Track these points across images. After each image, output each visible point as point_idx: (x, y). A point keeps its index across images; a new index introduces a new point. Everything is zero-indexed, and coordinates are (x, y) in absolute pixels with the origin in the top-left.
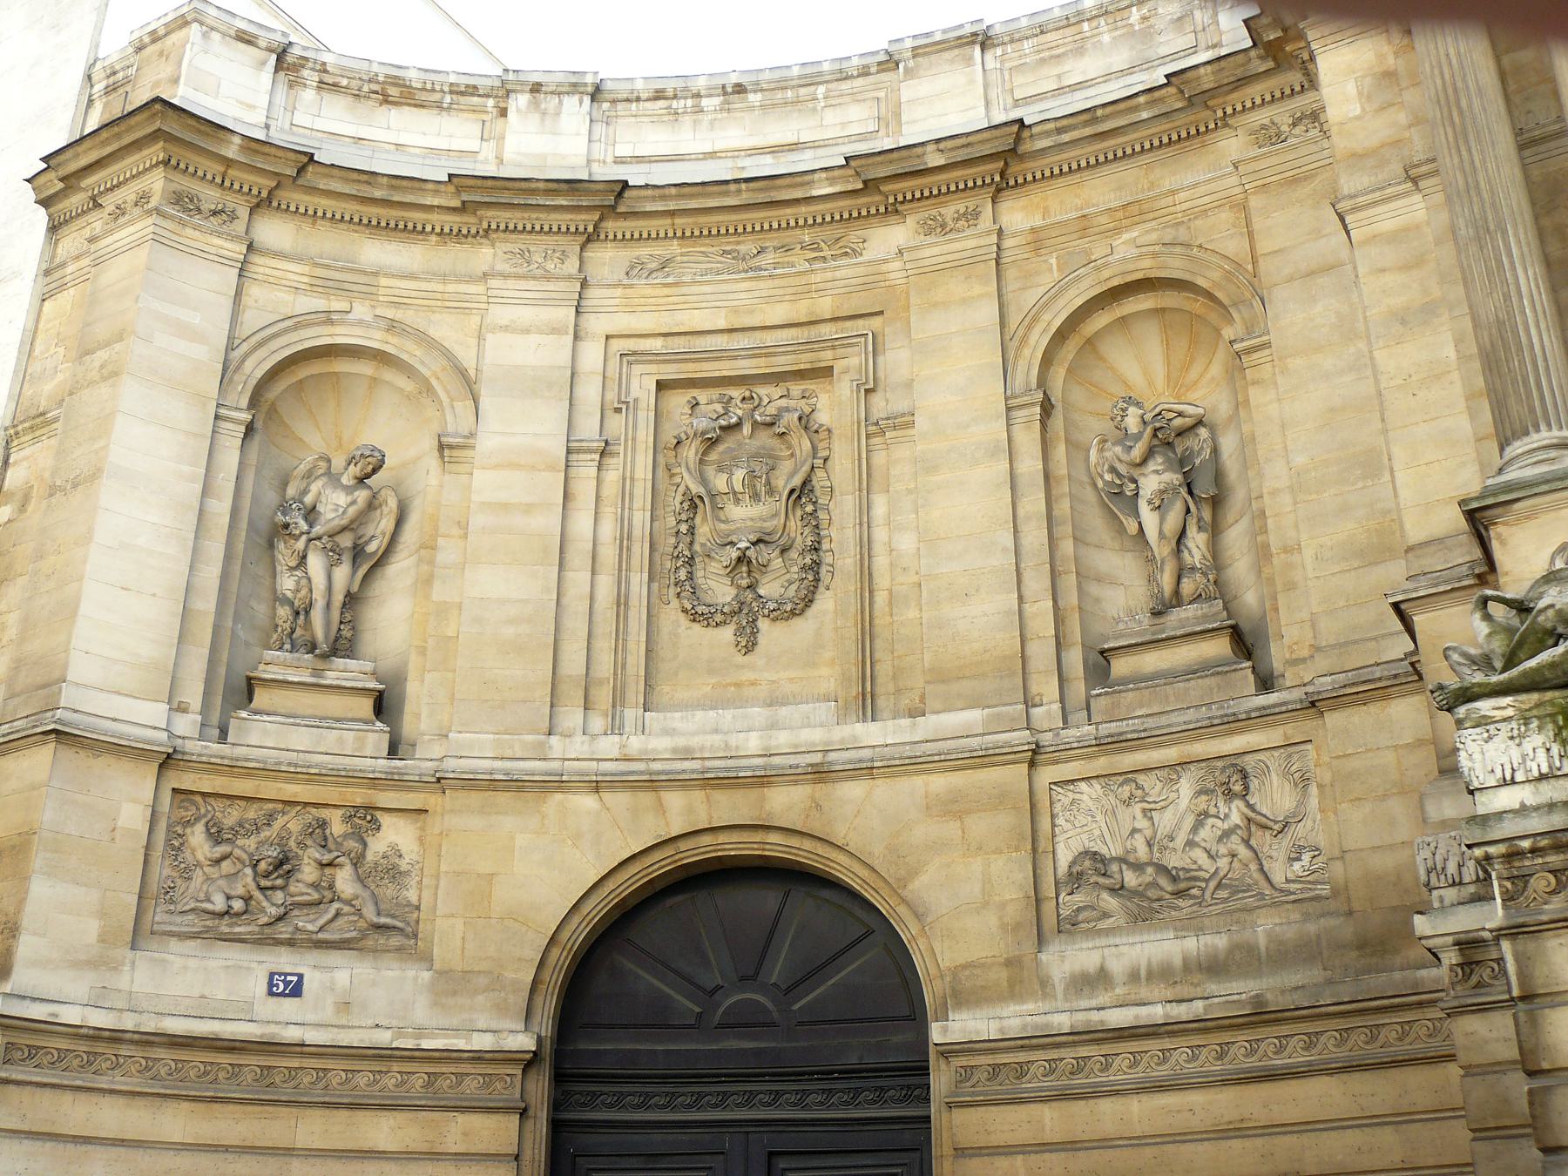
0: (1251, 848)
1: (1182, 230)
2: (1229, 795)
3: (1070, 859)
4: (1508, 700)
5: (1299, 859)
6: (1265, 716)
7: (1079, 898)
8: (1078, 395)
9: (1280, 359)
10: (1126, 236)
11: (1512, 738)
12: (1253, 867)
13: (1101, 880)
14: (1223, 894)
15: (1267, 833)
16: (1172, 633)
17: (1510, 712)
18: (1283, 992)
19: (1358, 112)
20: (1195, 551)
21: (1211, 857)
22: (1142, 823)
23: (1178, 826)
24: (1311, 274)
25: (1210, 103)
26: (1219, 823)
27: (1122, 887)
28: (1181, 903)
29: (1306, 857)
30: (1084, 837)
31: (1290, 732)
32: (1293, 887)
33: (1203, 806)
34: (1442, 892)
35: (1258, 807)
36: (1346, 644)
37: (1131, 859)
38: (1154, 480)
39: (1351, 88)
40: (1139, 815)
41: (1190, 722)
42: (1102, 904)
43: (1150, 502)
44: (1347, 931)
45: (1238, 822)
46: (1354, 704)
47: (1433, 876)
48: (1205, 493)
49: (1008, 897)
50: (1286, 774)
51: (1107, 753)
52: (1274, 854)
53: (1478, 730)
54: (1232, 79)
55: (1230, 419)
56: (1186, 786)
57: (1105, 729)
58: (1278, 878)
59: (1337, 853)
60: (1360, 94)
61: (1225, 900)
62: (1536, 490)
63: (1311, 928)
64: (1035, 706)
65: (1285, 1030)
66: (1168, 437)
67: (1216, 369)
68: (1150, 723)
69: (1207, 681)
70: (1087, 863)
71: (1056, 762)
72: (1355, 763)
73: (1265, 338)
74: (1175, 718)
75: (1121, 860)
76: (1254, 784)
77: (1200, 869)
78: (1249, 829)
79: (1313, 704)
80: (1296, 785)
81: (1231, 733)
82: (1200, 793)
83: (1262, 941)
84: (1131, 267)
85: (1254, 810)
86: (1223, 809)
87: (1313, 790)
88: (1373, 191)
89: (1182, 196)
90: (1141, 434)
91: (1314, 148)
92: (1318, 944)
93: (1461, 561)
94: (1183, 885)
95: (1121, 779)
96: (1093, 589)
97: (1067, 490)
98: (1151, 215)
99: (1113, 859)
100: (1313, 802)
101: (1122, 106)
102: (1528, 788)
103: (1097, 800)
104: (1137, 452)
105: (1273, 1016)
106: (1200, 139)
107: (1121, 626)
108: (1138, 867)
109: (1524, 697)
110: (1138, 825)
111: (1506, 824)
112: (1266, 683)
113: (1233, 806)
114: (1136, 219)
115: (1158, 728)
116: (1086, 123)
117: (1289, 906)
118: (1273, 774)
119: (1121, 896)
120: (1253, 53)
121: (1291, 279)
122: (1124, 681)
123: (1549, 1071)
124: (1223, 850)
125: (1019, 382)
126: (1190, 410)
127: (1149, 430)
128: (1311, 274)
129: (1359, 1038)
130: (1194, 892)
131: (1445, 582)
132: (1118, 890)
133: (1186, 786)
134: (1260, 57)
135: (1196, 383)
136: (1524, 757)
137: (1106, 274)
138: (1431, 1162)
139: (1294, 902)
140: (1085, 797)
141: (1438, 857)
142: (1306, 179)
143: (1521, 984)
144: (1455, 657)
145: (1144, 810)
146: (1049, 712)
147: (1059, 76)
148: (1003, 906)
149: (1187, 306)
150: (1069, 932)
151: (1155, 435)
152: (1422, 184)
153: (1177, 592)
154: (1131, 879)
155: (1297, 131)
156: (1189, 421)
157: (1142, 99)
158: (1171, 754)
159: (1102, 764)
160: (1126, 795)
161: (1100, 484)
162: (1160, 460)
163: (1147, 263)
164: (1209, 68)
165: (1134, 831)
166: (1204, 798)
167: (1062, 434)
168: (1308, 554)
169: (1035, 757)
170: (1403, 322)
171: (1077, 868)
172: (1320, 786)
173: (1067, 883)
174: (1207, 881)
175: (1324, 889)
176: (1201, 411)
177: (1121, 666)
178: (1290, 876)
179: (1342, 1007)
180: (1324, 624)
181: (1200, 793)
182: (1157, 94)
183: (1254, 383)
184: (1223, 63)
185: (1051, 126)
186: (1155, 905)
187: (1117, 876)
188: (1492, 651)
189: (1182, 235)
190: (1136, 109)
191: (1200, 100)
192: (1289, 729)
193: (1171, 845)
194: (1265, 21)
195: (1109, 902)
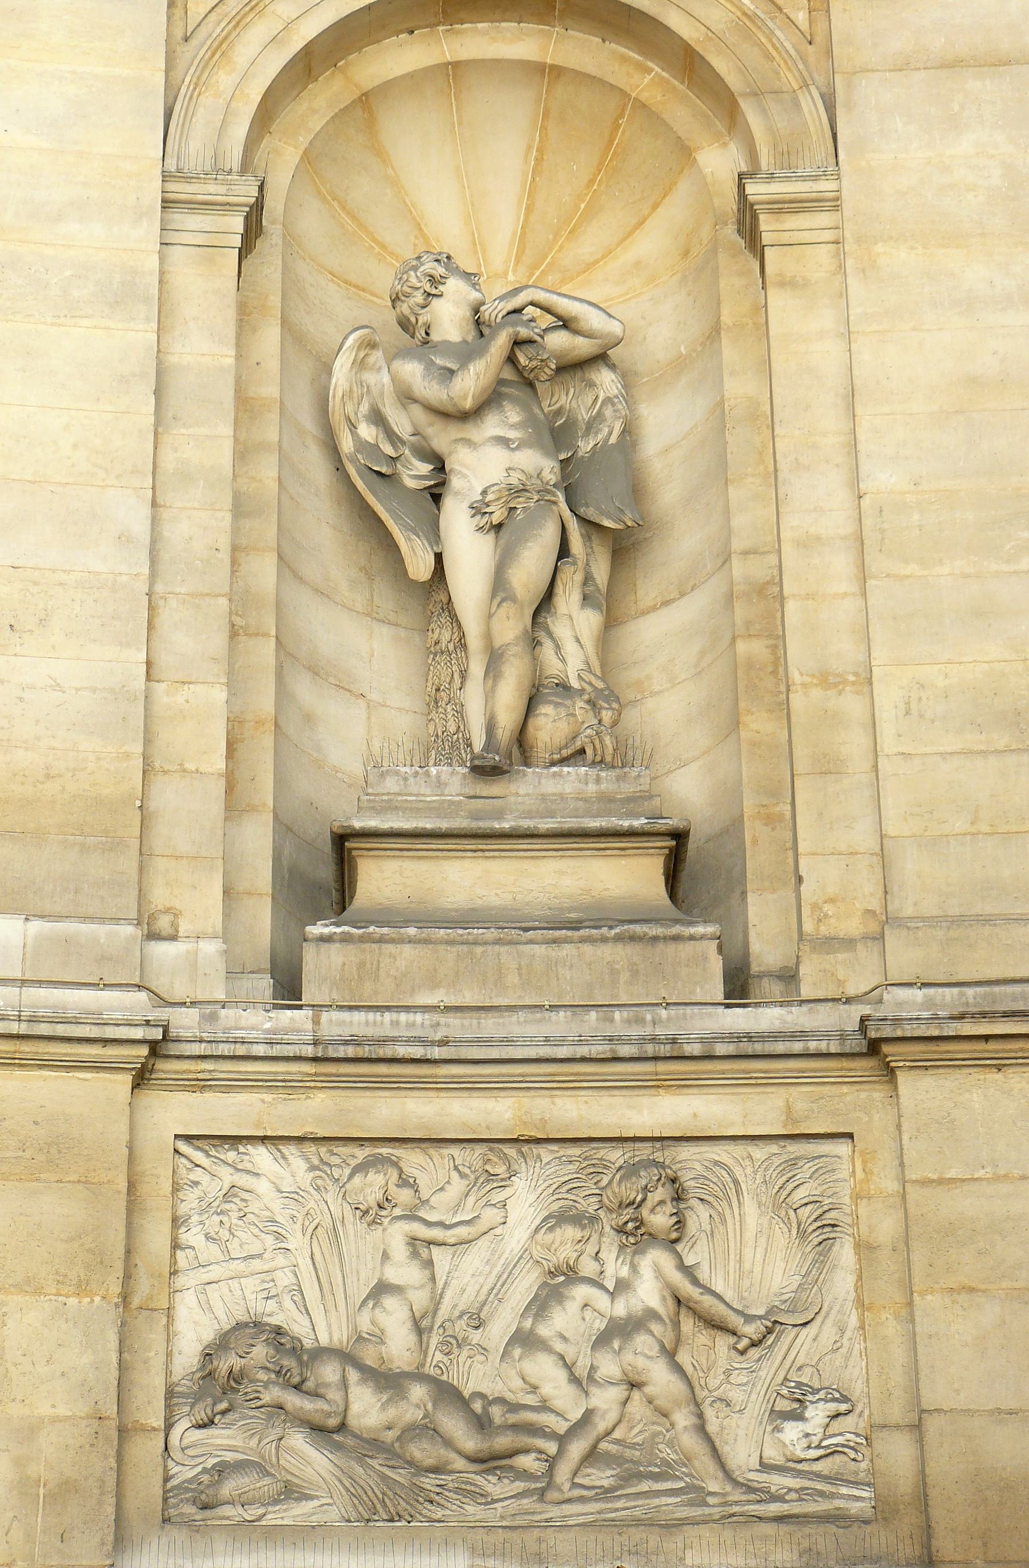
0: (678, 1369)
2: (635, 1235)
3: (208, 1334)
5: (797, 1416)
7: (227, 1440)
8: (313, 223)
9: (859, 240)
12: (683, 1419)
13: (293, 1400)
14: (602, 1477)
15: (724, 1342)
16: (527, 824)
20: (570, 648)
21: (575, 1380)
22: (404, 1272)
23: (497, 1292)
24: (953, 64)
26: (602, 1301)
27: (342, 1427)
28: (492, 1485)
29: (817, 1414)
30: (251, 1285)
31: (800, 1106)
32: (778, 1482)
33: (566, 1253)
35: (703, 1275)
36: (959, 921)
37: (369, 1356)
38: (489, 461)
40: (399, 1250)
41: (561, 1041)
42: (287, 1461)
43: (478, 510)
45: (654, 1301)
46: (977, 1063)
48: (600, 522)
49: (44, 1409)
51: (333, 1084)
52: (736, 1395)
55: (680, 365)
56: (527, 1197)
57: (337, 1024)
58: (742, 1456)
59: (897, 1412)
61: (606, 1493)
64: (153, 936)
66: (537, 367)
67: (653, 243)
68: (454, 1026)
69: (609, 952)
70: (260, 1352)
71: (201, 1085)
72: (965, 1204)
73: (826, 186)
74: (515, 1025)
75: (347, 1357)
76: (698, 1217)
77: (544, 1407)
78: (677, 1325)
79: (874, 1047)
80: (802, 1234)
81: (658, 1084)
82: (560, 1218)
85: (695, 1282)
86: (615, 1268)
87: (845, 1253)
90: (466, 353)
94: (503, 1442)
95: (361, 1154)
96: (305, 690)
97: (272, 434)
99: (320, 1353)
100: (842, 1283)
103: (294, 1196)
104: (470, 383)
107: (391, 785)
108: (389, 1381)
110: (393, 1275)
112: (738, 986)
115: (479, 1042)
117: (769, 1529)
118: (747, 1199)
119: (339, 1447)
121: (903, 66)
122: (391, 917)
124: (609, 1367)
125: (195, 146)
126: (594, 320)
127: (501, 343)
128: (953, 64)
130: (527, 1462)
132: (328, 1432)
133: (527, 1197)
135: (590, 266)
140: (262, 1186)
145: (413, 1241)
146: (192, 963)
148: (29, 1431)
149: (618, 75)
150: (188, 1523)
151: (511, 359)
153: (521, 738)
154: (367, 1408)
156: (583, 346)
158: (497, 1112)
159: (317, 1109)
160: (372, 1197)
161: (347, 445)
162: (513, 414)
165: (382, 1289)
166: (571, 1232)
167: (275, 300)
168: (888, 697)
169: (153, 1059)
171: (226, 1363)
172: (864, 1248)
173: (197, 1398)
174: (563, 1440)
175: (858, 1501)
177: (380, 879)
178: (773, 1455)
180: (911, 865)
181: (560, 1218)
183: (787, 283)
186: (429, 1482)
187: (335, 1395)
192: (800, 1097)
193: (476, 1337)
195: (308, 1459)
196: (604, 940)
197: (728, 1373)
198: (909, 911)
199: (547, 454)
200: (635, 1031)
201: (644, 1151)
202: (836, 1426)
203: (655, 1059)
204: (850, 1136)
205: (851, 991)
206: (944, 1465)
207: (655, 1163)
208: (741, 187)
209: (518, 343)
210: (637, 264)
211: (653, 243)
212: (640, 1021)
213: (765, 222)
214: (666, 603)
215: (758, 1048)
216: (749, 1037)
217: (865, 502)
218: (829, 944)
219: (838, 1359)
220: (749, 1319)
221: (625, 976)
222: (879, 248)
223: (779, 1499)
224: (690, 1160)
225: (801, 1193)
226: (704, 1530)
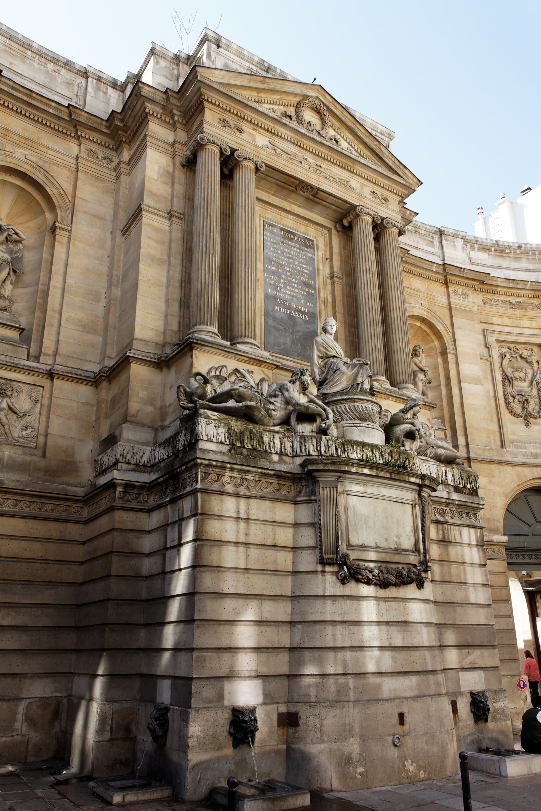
0: (7, 418)
1: (47, 165)
4: (216, 414)
6: (29, 371)
10: (22, 151)
11: (215, 427)
15: (15, 416)
17: (216, 418)
18: (13, 481)
19: (156, 178)
25: (78, 127)
29: (29, 430)
32: (21, 440)
34: (122, 464)
36: (69, 356)
39: (156, 168)
44: (42, 463)
47: (122, 457)
50: (30, 396)
52: (16, 425)
53: (206, 420)
54: (92, 125)
58: (16, 434)
60: (158, 173)
62: (213, 346)
63: (28, 458)
65: (7, 496)
69: (7, 346)
76: (15, 394)
80: (32, 401)
83: (6, 458)
84: (21, 164)
87: (39, 405)
88: (156, 209)
89: (51, 152)
91: (108, 172)
92: (29, 465)
93: (151, 351)
98: (35, 150)
100: (37, 410)
101: (45, 100)
102: (216, 444)
105: (5, 489)
106: (65, 136)
109: (221, 414)
111: (210, 454)
113: (5, 400)
114: (29, 147)
116: (26, 95)
117: (18, 447)
120: (104, 123)
121: (86, 213)
123: (204, 540)
126: (22, 235)
129: (49, 507)
131: (148, 357)
134: (106, 126)
136: (218, 434)
137: (9, 160)
138: (52, 558)
139: (20, 446)
141: (125, 451)
142: (102, 181)
143: (202, 509)
144: (182, 389)
147: (11, 63)
152: (173, 219)
155: (104, 161)
156: (17, 238)
157: (53, 104)
162: (5, 247)
163: (28, 168)
164: (86, 115)
170: (152, 260)
176: (24, 237)
179: (53, 495)
182: (60, 107)
184: (92, 117)
185: (11, 84)
188: (196, 393)
189: (46, 167)
190: (49, 106)
191: (76, 124)
192: (36, 379)
194: (119, 116)
196: (7, 344)
197: (15, 421)
198: (61, 353)
199: (9, 256)
200: (11, 361)
201: (8, 381)
202: (32, 433)
203: (13, 366)
204: (43, 387)
205: (48, 363)
206: (50, 442)
207: (9, 384)
208: (54, 223)
209: (8, 235)
210: (29, 227)
211: (32, 224)
212: (11, 359)
213: (57, 230)
214: (23, 288)
215: (32, 369)
216: (30, 367)
217: (66, 284)
218: (46, 355)
219: (34, 422)
220: (21, 413)
221: (10, 351)
222: (76, 242)
223: (20, 443)
224: (15, 385)
225: (33, 394)
226: (7, 446)
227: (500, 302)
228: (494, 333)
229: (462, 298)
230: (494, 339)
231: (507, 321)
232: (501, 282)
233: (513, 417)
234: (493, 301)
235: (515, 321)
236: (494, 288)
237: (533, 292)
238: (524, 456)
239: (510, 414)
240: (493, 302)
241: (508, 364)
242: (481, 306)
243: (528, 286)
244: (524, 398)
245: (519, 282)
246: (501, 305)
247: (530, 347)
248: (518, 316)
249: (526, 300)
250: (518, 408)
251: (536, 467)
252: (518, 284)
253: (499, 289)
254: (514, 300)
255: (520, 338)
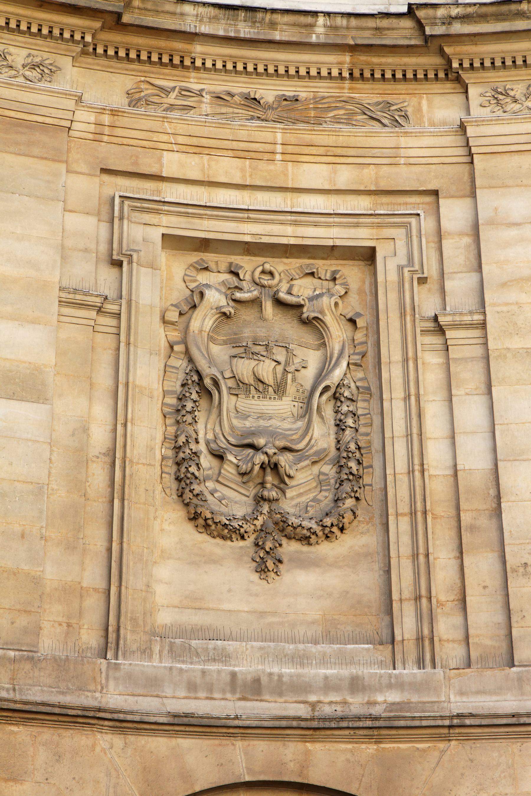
227: (207, 98)
228: (158, 212)
229: (21, 80)
230: (156, 234)
231: (226, 168)
232: (200, 18)
233: (205, 537)
234: (173, 95)
235: (262, 165)
236: (179, 45)
237: (347, 58)
238: (192, 687)
239: (189, 527)
240: (172, 99)
241: (215, 329)
242: (114, 112)
243: (319, 32)
244: (260, 458)
245: (278, 17)
246: (206, 108)
247: (325, 267)
248: (279, 148)
249: (324, 89)
250: (232, 500)
251: (244, 736)
252: (273, 25)
253: (198, 48)
254: (268, 91)
255: (276, 229)
